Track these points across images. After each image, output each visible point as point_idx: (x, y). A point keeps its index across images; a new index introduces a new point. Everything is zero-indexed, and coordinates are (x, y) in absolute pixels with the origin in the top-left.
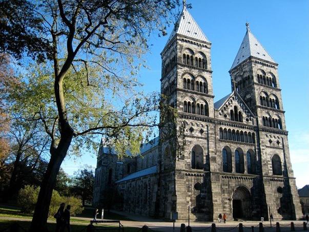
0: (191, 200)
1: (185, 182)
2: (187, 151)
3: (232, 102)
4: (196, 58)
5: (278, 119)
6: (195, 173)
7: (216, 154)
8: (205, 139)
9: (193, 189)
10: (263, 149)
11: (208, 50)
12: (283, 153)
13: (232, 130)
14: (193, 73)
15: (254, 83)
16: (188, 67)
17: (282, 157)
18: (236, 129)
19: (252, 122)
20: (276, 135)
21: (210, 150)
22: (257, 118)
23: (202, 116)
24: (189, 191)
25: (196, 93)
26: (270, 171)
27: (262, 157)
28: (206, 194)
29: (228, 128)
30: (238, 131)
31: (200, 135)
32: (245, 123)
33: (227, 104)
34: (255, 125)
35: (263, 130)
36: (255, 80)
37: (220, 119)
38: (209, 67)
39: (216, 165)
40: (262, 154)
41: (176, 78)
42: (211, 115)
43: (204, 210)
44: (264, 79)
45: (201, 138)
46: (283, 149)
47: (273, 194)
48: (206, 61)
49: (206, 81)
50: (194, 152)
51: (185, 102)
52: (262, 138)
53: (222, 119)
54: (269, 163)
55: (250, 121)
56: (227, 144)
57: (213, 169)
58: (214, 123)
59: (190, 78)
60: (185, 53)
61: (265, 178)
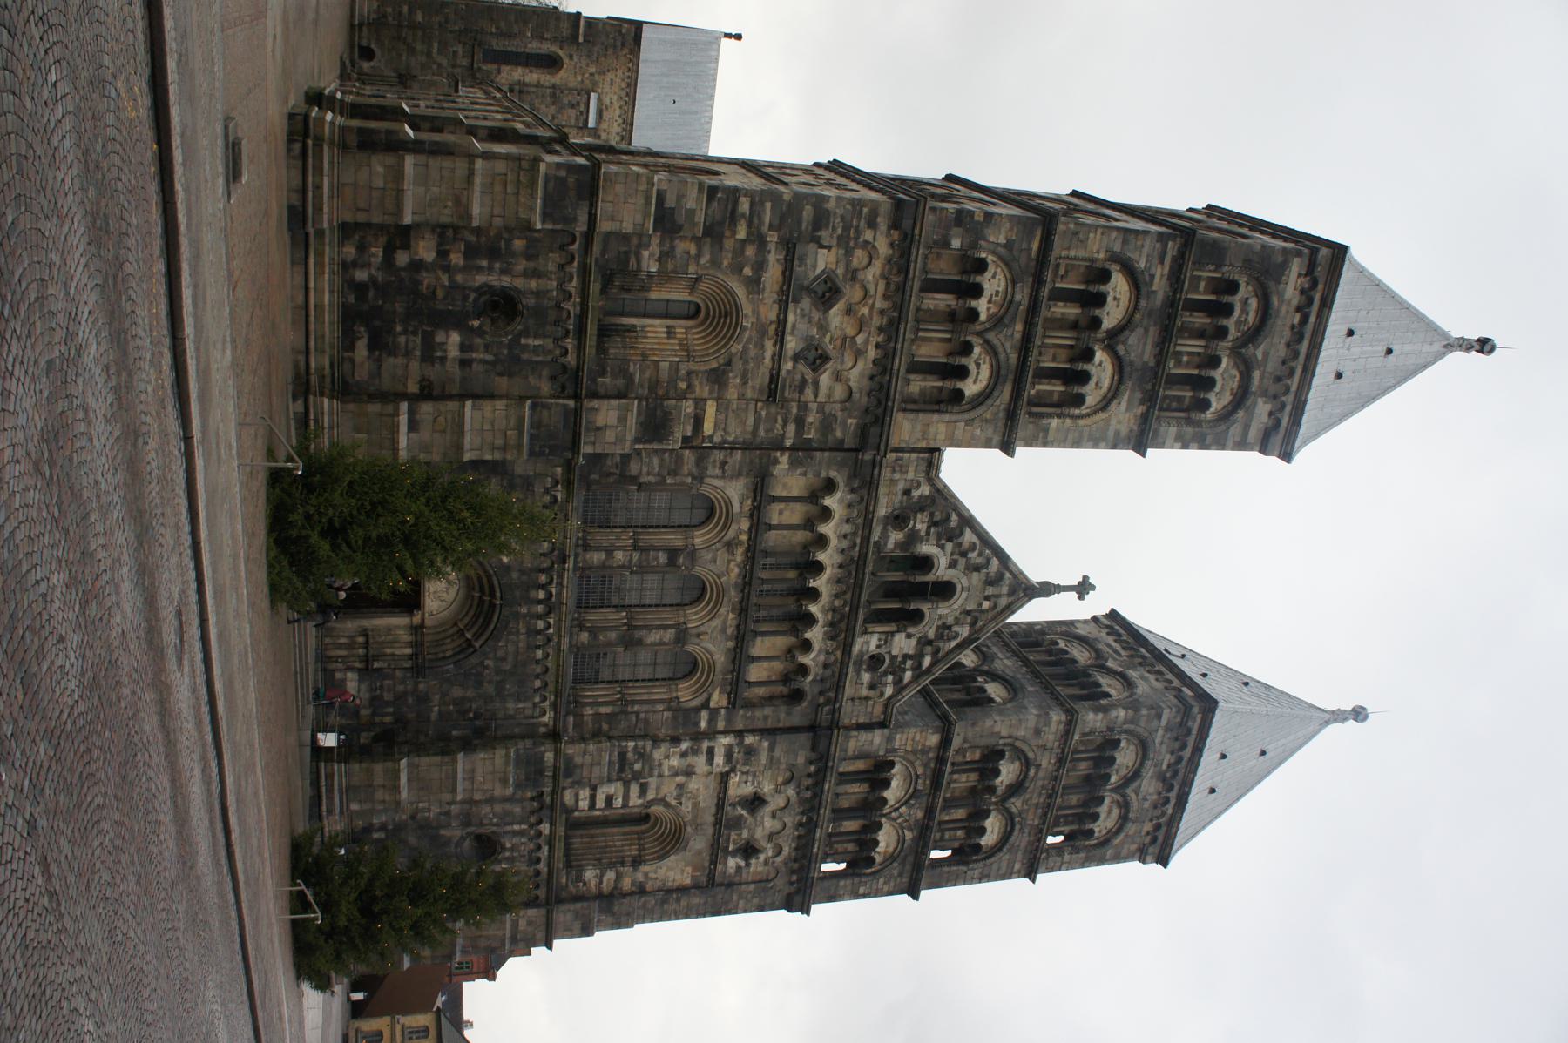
0: (417, 266)
1: (527, 227)
3: (977, 568)
8: (774, 378)
10: (711, 753)
12: (688, 881)
14: (1140, 331)
17: (674, 870)
18: (821, 583)
19: (865, 692)
22: (882, 725)
25: (1027, 338)
30: (814, 594)
31: (792, 344)
32: (856, 649)
33: (968, 537)
34: (851, 713)
35: (822, 760)
39: (620, 440)
40: (685, 746)
43: (361, 351)
45: (778, 357)
48: (1198, 424)
49: (1088, 415)
52: (772, 748)
53: (883, 500)
54: (634, 789)
59: (1111, 316)
60: (1243, 291)
61: (549, 756)
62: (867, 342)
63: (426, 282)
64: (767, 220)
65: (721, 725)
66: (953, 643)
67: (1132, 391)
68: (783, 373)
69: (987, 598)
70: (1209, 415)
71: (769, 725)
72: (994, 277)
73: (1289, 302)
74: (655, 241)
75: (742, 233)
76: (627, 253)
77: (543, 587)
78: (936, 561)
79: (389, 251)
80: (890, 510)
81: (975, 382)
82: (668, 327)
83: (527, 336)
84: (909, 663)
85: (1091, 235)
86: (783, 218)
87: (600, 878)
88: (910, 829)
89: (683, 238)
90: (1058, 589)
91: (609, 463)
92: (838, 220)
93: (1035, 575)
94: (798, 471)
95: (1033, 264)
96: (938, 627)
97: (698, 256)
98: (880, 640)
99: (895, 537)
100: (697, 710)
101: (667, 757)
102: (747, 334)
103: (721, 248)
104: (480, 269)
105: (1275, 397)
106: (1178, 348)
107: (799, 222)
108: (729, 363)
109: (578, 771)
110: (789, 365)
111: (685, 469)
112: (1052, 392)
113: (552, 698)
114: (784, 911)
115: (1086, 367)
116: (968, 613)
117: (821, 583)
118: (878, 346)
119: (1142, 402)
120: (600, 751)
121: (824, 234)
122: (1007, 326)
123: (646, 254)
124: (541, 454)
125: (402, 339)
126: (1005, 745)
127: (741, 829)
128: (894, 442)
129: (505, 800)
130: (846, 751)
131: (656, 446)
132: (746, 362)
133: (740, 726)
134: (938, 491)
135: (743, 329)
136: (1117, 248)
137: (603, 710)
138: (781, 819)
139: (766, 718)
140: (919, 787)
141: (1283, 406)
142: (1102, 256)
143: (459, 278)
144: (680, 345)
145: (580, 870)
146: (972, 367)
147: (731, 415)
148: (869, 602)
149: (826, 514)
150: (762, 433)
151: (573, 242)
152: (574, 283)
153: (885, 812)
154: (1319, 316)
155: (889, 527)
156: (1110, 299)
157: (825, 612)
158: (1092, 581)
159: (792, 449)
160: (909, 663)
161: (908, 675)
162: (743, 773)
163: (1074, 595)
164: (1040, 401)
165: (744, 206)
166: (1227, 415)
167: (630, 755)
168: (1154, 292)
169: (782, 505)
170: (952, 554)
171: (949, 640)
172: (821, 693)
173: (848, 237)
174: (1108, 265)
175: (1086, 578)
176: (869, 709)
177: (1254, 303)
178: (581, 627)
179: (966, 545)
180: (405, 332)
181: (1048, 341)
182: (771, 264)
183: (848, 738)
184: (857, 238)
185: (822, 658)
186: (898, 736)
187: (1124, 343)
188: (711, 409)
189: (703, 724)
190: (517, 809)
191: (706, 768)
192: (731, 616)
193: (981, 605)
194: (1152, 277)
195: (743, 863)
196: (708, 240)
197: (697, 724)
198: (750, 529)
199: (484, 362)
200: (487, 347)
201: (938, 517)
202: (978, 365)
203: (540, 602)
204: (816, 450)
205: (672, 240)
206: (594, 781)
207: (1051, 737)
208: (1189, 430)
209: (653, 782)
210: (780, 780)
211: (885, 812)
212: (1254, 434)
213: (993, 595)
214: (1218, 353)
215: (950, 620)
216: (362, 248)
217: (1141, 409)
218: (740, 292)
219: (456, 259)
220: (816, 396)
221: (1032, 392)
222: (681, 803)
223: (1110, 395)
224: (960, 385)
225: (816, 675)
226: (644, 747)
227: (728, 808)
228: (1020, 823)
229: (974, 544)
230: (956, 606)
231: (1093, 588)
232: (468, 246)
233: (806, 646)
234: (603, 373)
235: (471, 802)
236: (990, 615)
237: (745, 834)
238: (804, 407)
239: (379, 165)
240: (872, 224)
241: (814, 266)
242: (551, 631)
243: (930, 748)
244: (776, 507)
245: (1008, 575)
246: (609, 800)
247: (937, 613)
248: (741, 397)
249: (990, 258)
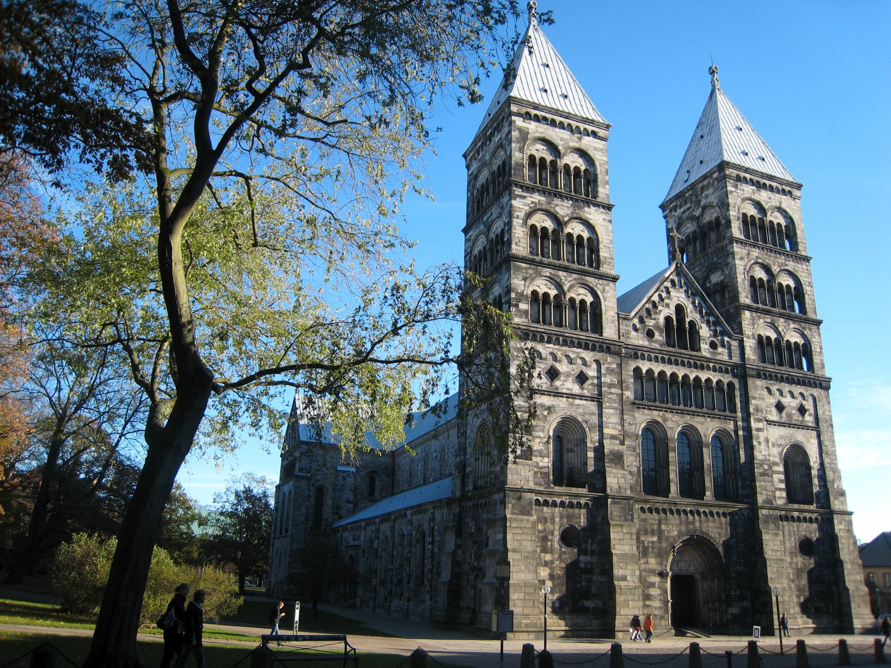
2: (542, 435)
4: (567, 167)
5: (801, 341)
6: (564, 498)
7: (622, 443)
8: (592, 399)
9: (556, 545)
10: (758, 430)
11: (600, 144)
13: (668, 374)
15: (732, 240)
16: (543, 192)
20: (798, 390)
21: (606, 431)
23: (583, 335)
24: (545, 550)
26: (778, 493)
27: (756, 453)
28: (595, 559)
29: (657, 368)
30: (685, 377)
36: (736, 231)
37: (636, 342)
38: (603, 192)
39: (624, 477)
40: (755, 443)
41: (509, 224)
42: (609, 332)
43: (589, 604)
44: (762, 227)
45: (581, 397)
46: (817, 428)
48: (596, 175)
50: (559, 438)
51: (535, 293)
52: (755, 398)
53: (641, 343)
56: (656, 415)
57: (616, 486)
58: (618, 354)
68: (589, 395)
81: (587, 296)
83: (580, 523)
91: (632, 482)
108: (586, 422)
111: (633, 443)
115: (575, 237)
119: (589, 207)
124: (632, 515)
128: (616, 337)
131: (625, 458)
132: (585, 413)
134: (636, 315)
144: (577, 445)
146: (580, 297)
147: (609, 421)
150: (616, 405)
157: (692, 372)
159: (622, 390)
180: (580, 583)
195: (808, 413)
198: (656, 410)
199: (592, 544)
200: (585, 542)
202: (579, 294)
209: (772, 459)
227: (783, 420)
233: (708, 380)
247: (692, 315)
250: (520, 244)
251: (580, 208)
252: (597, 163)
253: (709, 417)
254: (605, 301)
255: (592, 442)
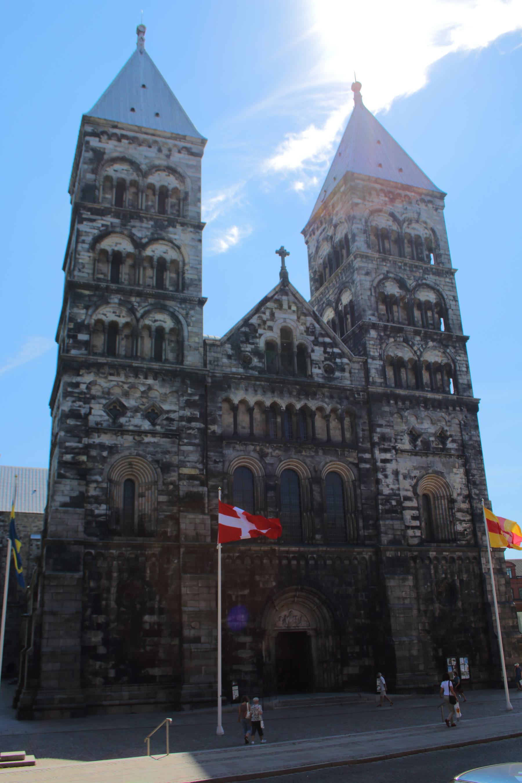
0: (106, 642)
3: (272, 314)
7: (203, 484)
14: (134, 231)
18: (283, 404)
19: (347, 374)
22: (366, 363)
25: (139, 294)
30: (290, 407)
32: (321, 380)
33: (254, 321)
37: (228, 370)
40: (380, 476)
43: (156, 672)
45: (154, 434)
47: (422, 607)
48: (187, 194)
49: (183, 256)
52: (381, 426)
53: (234, 370)
54: (407, 504)
55: (337, 374)
62: (144, 384)
63: (115, 636)
64: (74, 444)
65: (367, 456)
66: (317, 326)
67: (168, 232)
68: (163, 431)
69: (290, 308)
70: (181, 188)
71: (367, 428)
72: (105, 315)
73: (115, 146)
74: (89, 507)
75: (84, 458)
76: (97, 522)
77: (289, 562)
78: (269, 339)
79: (98, 657)
80: (240, 366)
81: (165, 322)
82: (139, 497)
84: (329, 350)
85: (80, 261)
86: (75, 436)
87: (461, 521)
88: (427, 343)
89: (87, 491)
90: (283, 268)
92: (75, 404)
93: (276, 281)
94: (219, 419)
95: (97, 293)
96: (308, 335)
97: (96, 482)
98: (316, 368)
99: (255, 361)
100: (359, 470)
101: (388, 486)
102: (141, 452)
103: (93, 469)
104: (107, 605)
105: (170, 150)
106: (144, 208)
107: (77, 426)
108: (157, 462)
109: (397, 537)
110: (158, 428)
112: (171, 278)
113: (355, 553)
114: (479, 414)
116: (299, 318)
117: (283, 404)
118: (146, 378)
119: (174, 227)
120: (385, 525)
121: (83, 411)
122: (133, 305)
123: (97, 512)
125: (148, 648)
126: (375, 292)
127: (429, 441)
129: (416, 578)
130: (381, 383)
132: (157, 452)
133: (368, 445)
134: (228, 339)
135: (138, 455)
136: (86, 246)
137: (361, 524)
138: (422, 419)
139: (363, 430)
140: (402, 339)
141: (175, 146)
142: (91, 254)
143: (112, 617)
145: (457, 533)
146: (157, 324)
147: (187, 459)
148: (294, 375)
149: (243, 402)
150: (197, 441)
151: (91, 553)
152: (114, 551)
153: (417, 359)
154: (123, 129)
155: (250, 366)
156: (116, 249)
157: (299, 400)
158: (278, 248)
159: (206, 423)
160: (329, 350)
161: (336, 350)
162: (396, 441)
163: (287, 258)
164: (176, 284)
165: (68, 457)
166: (181, 177)
167: (387, 507)
168: (112, 223)
169: (239, 427)
170: (265, 329)
171: (315, 328)
172: (347, 398)
173: (84, 398)
174: (97, 252)
175: (277, 252)
176: (356, 371)
177: (117, 166)
178: (313, 538)
179: (259, 322)
181: (141, 282)
182: (101, 441)
183: (374, 383)
184: (85, 393)
185: (327, 400)
186: (372, 354)
187: (141, 239)
188: (185, 471)
189: (368, 466)
190: (421, 571)
191: (394, 462)
192: (304, 453)
193: (294, 311)
194: (103, 225)
196: (88, 477)
197: (368, 470)
201: (243, 339)
202: (155, 321)
203: (298, 563)
204: (206, 410)
205: (89, 497)
206: (403, 527)
207: (370, 266)
208: (190, 199)
209: (403, 493)
210: (399, 420)
211: (417, 359)
212: (192, 161)
213: (289, 303)
214: (146, 184)
215: (302, 328)
216: (96, 674)
217: (178, 227)
218: (117, 457)
219: (101, 619)
220: (175, 411)
221: (171, 288)
222: (415, 477)
223: (170, 244)
224: (167, 330)
225: (337, 403)
226: (382, 499)
228: (422, 280)
229: (259, 317)
230: (295, 325)
231: (282, 248)
232: (93, 613)
233: (320, 409)
234: (165, 533)
235: (417, 599)
236: (299, 305)
237: (432, 439)
238: (182, 418)
239: (47, 666)
240: (77, 385)
241: (101, 416)
242: (315, 556)
243: (379, 335)
244: (240, 430)
245: (276, 297)
246: (414, 518)
248: (177, 453)
249: (95, 317)
250: (85, 270)
251: (163, 228)
252: (188, 181)
253: (322, 449)
254: (188, 325)
255: (164, 484)
